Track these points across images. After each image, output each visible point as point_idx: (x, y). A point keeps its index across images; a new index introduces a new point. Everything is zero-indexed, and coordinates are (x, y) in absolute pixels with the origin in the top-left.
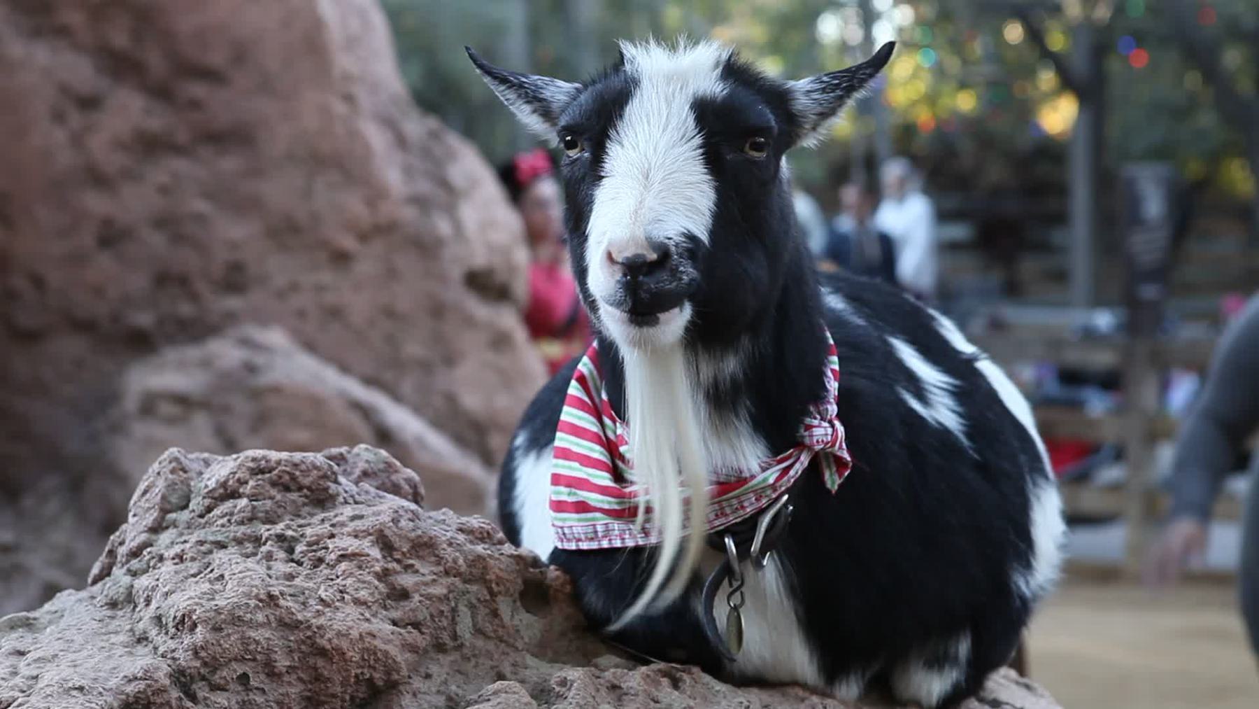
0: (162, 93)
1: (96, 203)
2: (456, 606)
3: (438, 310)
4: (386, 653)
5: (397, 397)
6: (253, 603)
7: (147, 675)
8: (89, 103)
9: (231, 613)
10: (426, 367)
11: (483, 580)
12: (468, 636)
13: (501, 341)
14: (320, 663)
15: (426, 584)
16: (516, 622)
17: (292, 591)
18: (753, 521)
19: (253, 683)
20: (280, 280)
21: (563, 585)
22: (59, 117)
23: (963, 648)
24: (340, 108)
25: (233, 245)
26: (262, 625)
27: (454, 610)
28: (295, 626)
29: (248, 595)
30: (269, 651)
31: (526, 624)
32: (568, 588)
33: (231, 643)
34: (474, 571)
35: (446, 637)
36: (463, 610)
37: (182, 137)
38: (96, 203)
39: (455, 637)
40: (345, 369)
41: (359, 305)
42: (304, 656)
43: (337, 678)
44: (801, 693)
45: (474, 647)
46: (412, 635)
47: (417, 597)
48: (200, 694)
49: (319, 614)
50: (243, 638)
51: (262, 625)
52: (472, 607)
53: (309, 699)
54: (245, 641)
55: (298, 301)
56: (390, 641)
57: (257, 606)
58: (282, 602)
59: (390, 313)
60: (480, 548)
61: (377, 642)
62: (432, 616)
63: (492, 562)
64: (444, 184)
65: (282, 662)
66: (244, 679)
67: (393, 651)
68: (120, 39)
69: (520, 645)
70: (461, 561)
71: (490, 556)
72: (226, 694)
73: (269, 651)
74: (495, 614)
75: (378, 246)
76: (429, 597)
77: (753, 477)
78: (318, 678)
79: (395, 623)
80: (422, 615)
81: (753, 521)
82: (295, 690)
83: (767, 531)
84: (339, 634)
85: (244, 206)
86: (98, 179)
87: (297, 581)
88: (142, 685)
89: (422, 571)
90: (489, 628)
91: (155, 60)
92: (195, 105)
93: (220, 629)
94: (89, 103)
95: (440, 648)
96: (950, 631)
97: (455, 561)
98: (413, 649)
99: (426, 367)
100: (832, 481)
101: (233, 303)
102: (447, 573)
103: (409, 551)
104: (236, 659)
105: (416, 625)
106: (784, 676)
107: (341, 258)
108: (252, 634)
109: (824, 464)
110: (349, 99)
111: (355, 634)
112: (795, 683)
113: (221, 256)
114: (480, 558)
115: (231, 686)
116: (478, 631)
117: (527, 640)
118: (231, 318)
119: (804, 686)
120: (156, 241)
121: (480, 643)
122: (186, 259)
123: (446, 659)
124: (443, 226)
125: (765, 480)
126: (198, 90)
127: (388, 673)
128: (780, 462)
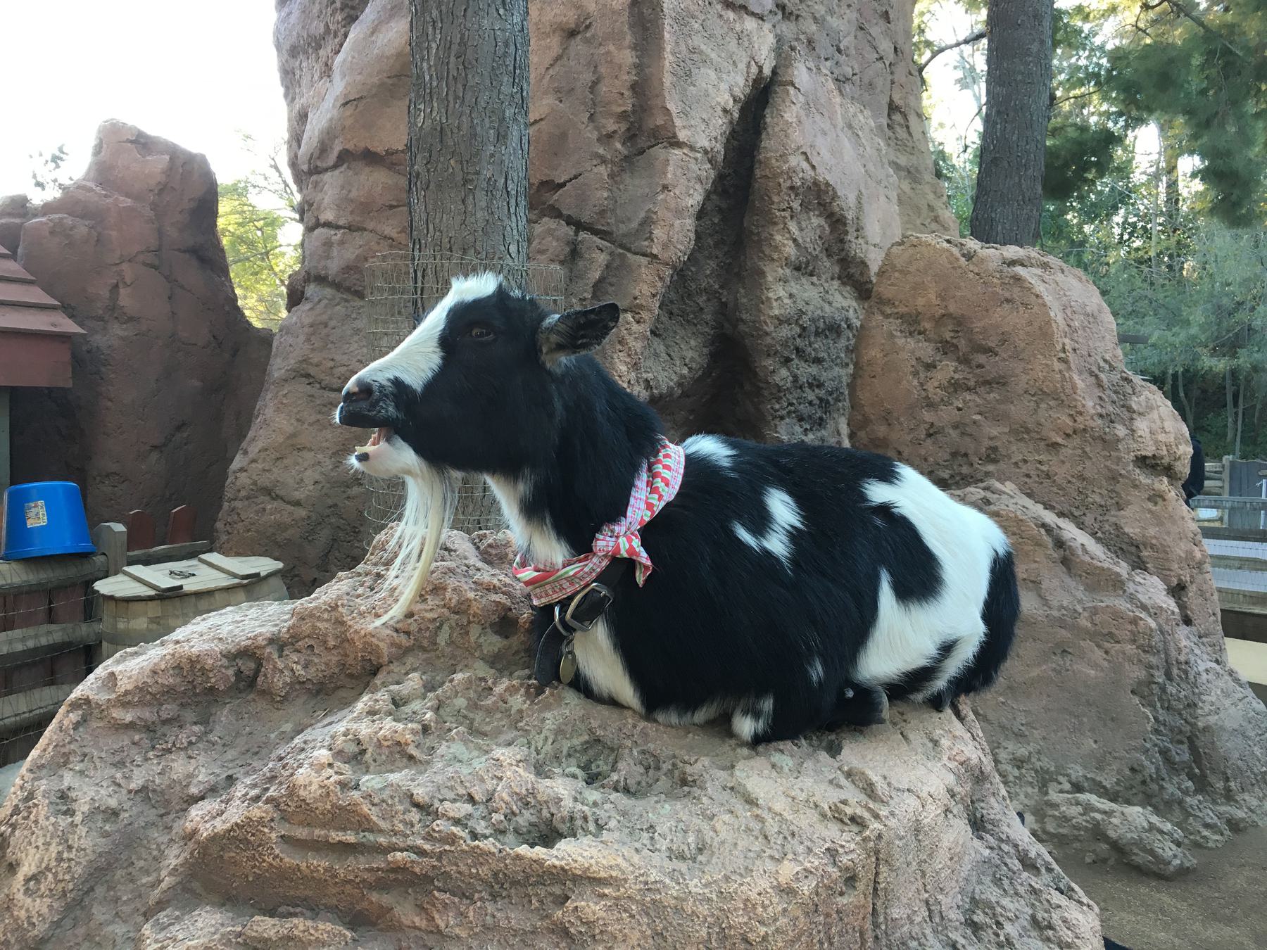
0: (964, 361)
1: (928, 416)
2: (441, 625)
3: (1114, 478)
4: (378, 646)
5: (1081, 526)
6: (324, 607)
7: (255, 638)
8: (930, 367)
9: (311, 611)
10: (1104, 509)
11: (465, 612)
12: (443, 643)
13: (1156, 497)
14: (346, 645)
15: (426, 611)
16: (482, 640)
17: (351, 603)
18: (570, 598)
19: (316, 651)
20: (1017, 457)
21: (525, 622)
22: (916, 374)
23: (768, 705)
24: (1057, 366)
25: (991, 439)
26: (327, 620)
27: (439, 628)
28: (343, 623)
29: (325, 603)
30: (325, 635)
31: (493, 643)
32: (527, 626)
33: (306, 628)
34: (463, 607)
35: (425, 643)
36: (446, 627)
37: (972, 383)
38: (928, 416)
39: (435, 644)
40: (1048, 507)
41: (1062, 472)
42: (342, 642)
43: (352, 656)
44: (630, 712)
45: (443, 649)
46: (403, 639)
47: (416, 617)
48: (285, 653)
49: (354, 618)
50: (313, 626)
51: (327, 620)
52: (451, 627)
53: (344, 665)
54: (314, 627)
55: (1024, 469)
56: (383, 640)
57: (326, 610)
58: (340, 609)
59: (1082, 478)
60: (471, 595)
61: (373, 639)
62: (420, 629)
63: (474, 603)
64: (1130, 410)
65: (331, 643)
66: (311, 647)
67: (381, 645)
68: (948, 336)
69: (477, 654)
70: (453, 601)
71: (475, 600)
72: (299, 655)
73: (325, 635)
74: (467, 633)
75: (1077, 441)
76: (423, 618)
77: (558, 570)
78: (346, 655)
79: (397, 631)
80: (414, 628)
81: (570, 598)
82: (335, 659)
83: (578, 607)
84: (356, 631)
85: (998, 417)
86: (931, 405)
87: (358, 600)
88: (250, 642)
89: (430, 603)
90: (459, 641)
91: (963, 344)
92: (980, 366)
93: (304, 619)
94: (930, 367)
95: (425, 650)
96: (760, 694)
97: (450, 600)
98: (399, 646)
99: (1104, 509)
100: (640, 578)
101: (991, 468)
102: (444, 606)
103: (431, 591)
104: (308, 636)
105: (408, 633)
106: (625, 704)
107: (1055, 445)
108: (318, 624)
109: (638, 566)
110: (1064, 361)
111: (363, 633)
112: (628, 708)
113: (987, 443)
114: (468, 600)
115: (304, 651)
116: (451, 643)
117: (485, 652)
118: (988, 474)
119: (634, 711)
120: (954, 434)
121: (448, 650)
122: (968, 445)
123: (422, 656)
124: (1121, 431)
125: (567, 573)
126: (981, 358)
127: (379, 658)
128: (580, 561)
